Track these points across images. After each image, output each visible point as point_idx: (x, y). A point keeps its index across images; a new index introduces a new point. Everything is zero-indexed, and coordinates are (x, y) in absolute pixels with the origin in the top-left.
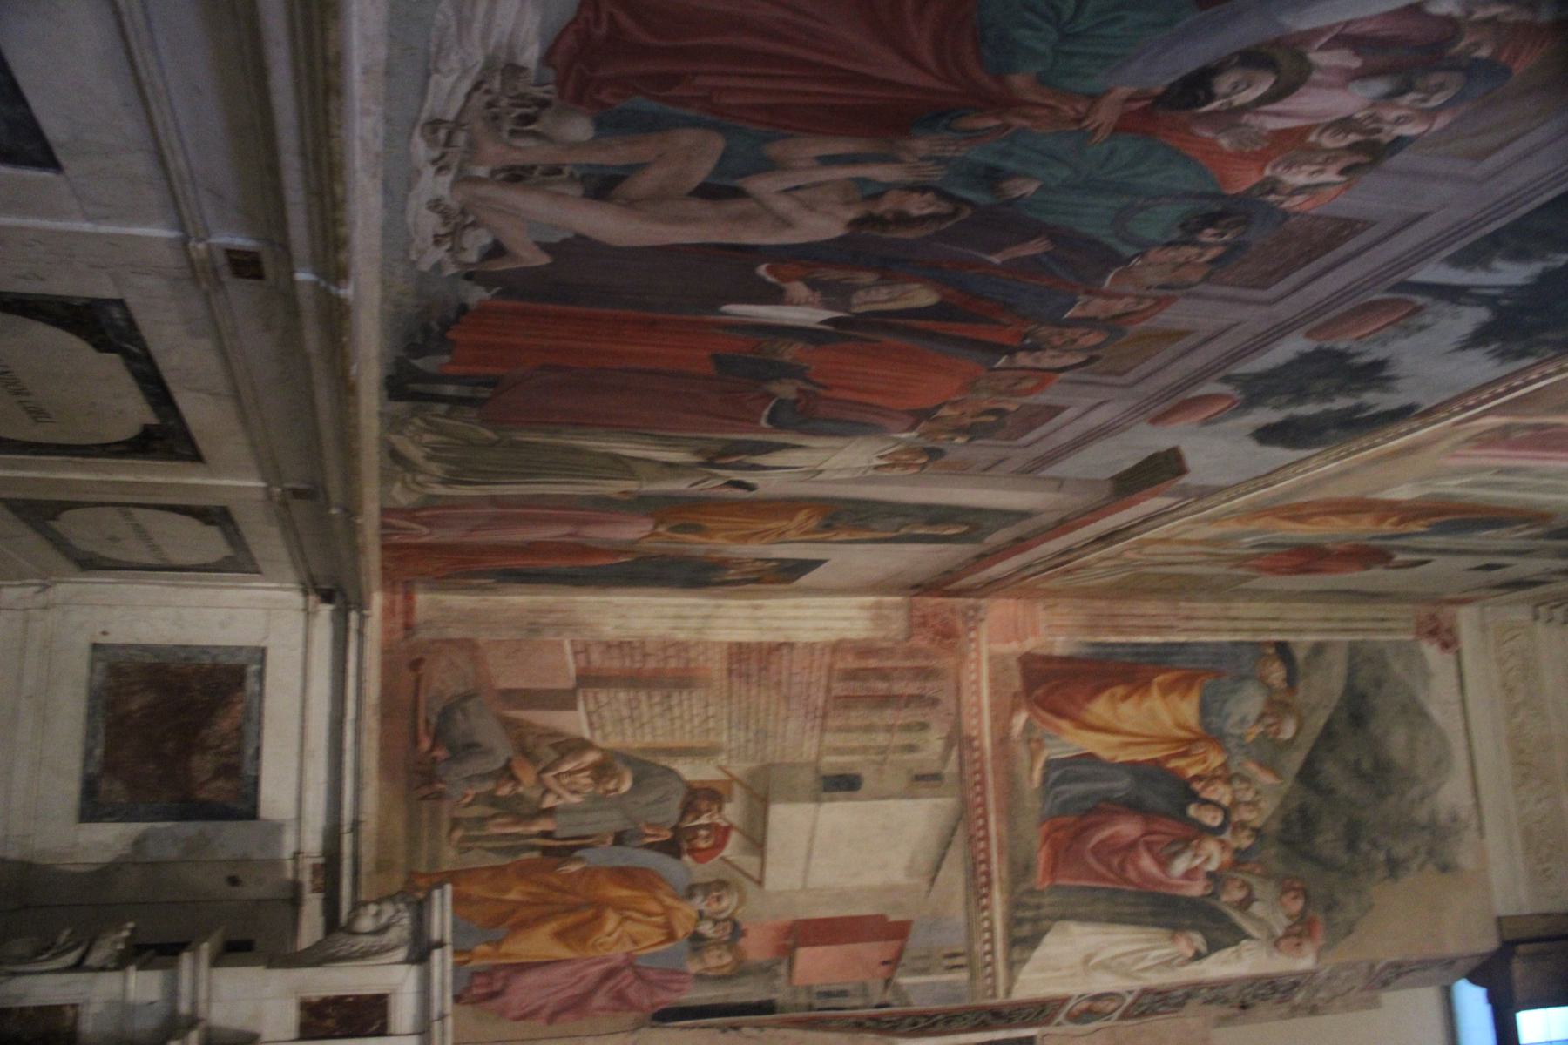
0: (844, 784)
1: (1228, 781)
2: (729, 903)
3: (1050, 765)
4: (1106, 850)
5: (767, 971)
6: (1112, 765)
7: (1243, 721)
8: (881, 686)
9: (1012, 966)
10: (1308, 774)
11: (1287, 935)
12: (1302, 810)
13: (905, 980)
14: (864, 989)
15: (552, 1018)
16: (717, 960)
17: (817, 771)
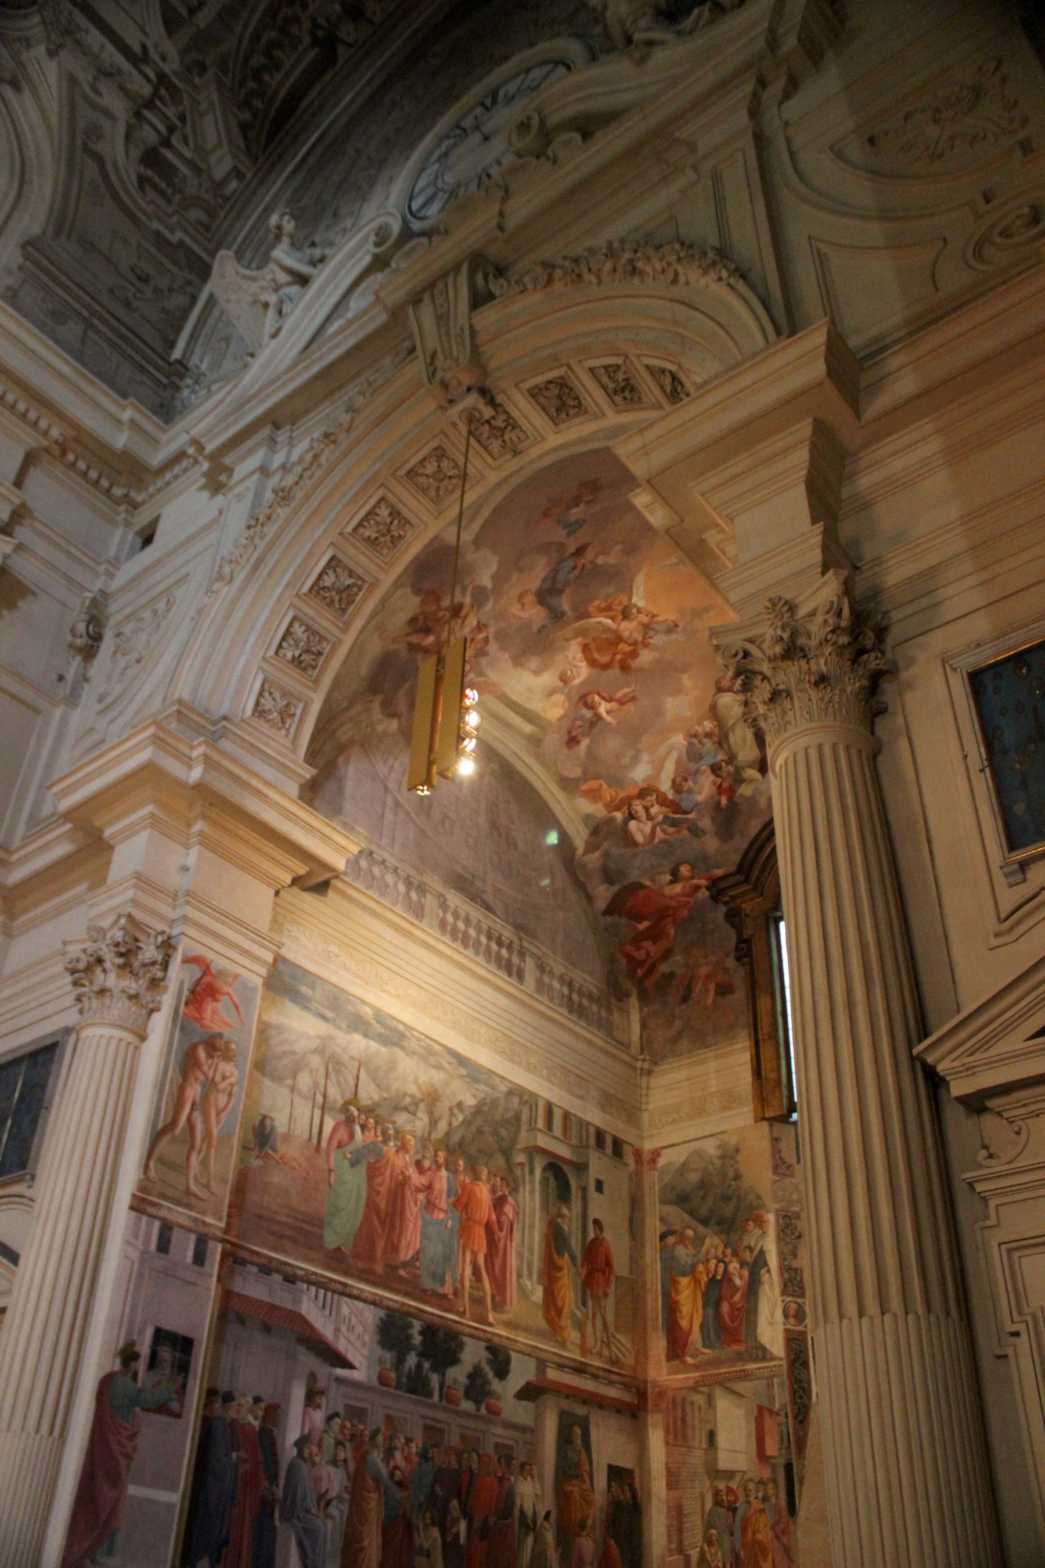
0: (712, 1436)
1: (708, 1260)
2: (751, 1486)
3: (704, 1346)
5: (774, 1468)
8: (679, 1423)
9: (773, 1358)
10: (705, 1222)
11: (761, 1228)
12: (718, 1224)
13: (777, 1406)
16: (771, 1492)
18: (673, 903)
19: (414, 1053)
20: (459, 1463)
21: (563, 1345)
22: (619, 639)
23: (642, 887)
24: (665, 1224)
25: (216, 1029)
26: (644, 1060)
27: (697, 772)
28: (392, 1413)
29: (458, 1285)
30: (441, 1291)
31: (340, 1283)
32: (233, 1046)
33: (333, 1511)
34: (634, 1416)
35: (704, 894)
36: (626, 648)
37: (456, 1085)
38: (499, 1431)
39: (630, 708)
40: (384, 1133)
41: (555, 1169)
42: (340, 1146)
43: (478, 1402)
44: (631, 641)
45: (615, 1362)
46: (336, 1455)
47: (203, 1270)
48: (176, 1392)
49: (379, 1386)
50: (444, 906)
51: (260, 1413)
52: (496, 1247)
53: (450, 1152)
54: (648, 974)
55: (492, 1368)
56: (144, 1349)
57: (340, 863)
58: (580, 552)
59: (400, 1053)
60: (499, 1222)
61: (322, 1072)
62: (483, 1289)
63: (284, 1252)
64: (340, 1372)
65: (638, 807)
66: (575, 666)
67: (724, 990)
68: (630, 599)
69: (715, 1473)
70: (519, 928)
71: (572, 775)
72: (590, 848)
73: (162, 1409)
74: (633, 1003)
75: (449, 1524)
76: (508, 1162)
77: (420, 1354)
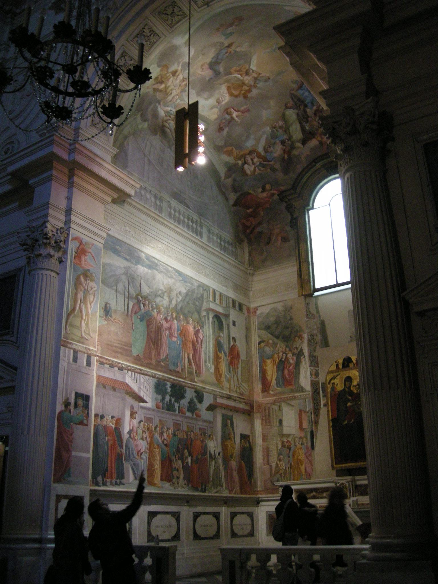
0: (281, 421)
1: (279, 353)
2: (297, 439)
3: (277, 387)
4: (289, 376)
5: (306, 432)
6: (277, 376)
7: (270, 351)
8: (267, 416)
10: (277, 337)
11: (301, 340)
13: (307, 409)
14: (308, 416)
15: (312, 465)
16: (305, 441)
17: (279, 427)
18: (262, 201)
19: (162, 272)
20: (187, 436)
21: (222, 388)
22: (243, 84)
23: (248, 193)
24: (261, 338)
25: (87, 268)
26: (251, 269)
27: (275, 143)
28: (162, 419)
29: (183, 367)
30: (177, 370)
31: (139, 369)
32: (94, 275)
33: (143, 456)
34: (249, 415)
35: (276, 197)
36: (246, 88)
37: (178, 284)
38: (201, 423)
39: (247, 114)
40: (152, 307)
41: (217, 317)
42: (136, 313)
43: (193, 413)
44: (248, 85)
45: (242, 394)
46: (143, 436)
47: (90, 368)
48: (85, 416)
49: (156, 409)
50: (170, 207)
51: (114, 422)
52: (196, 351)
53: (177, 313)
54: (251, 232)
55: (197, 399)
56: (72, 401)
57: (132, 192)
58: (229, 46)
59: (156, 272)
60: (197, 341)
61: (127, 283)
62: (193, 369)
63: (118, 358)
64: (142, 404)
65: (248, 158)
66: (224, 96)
67: (285, 240)
68: (250, 66)
69: (282, 435)
70: (200, 214)
71: (220, 144)
72: (227, 176)
73: (81, 423)
74: (246, 245)
75: (184, 459)
76: (199, 316)
77: (170, 396)
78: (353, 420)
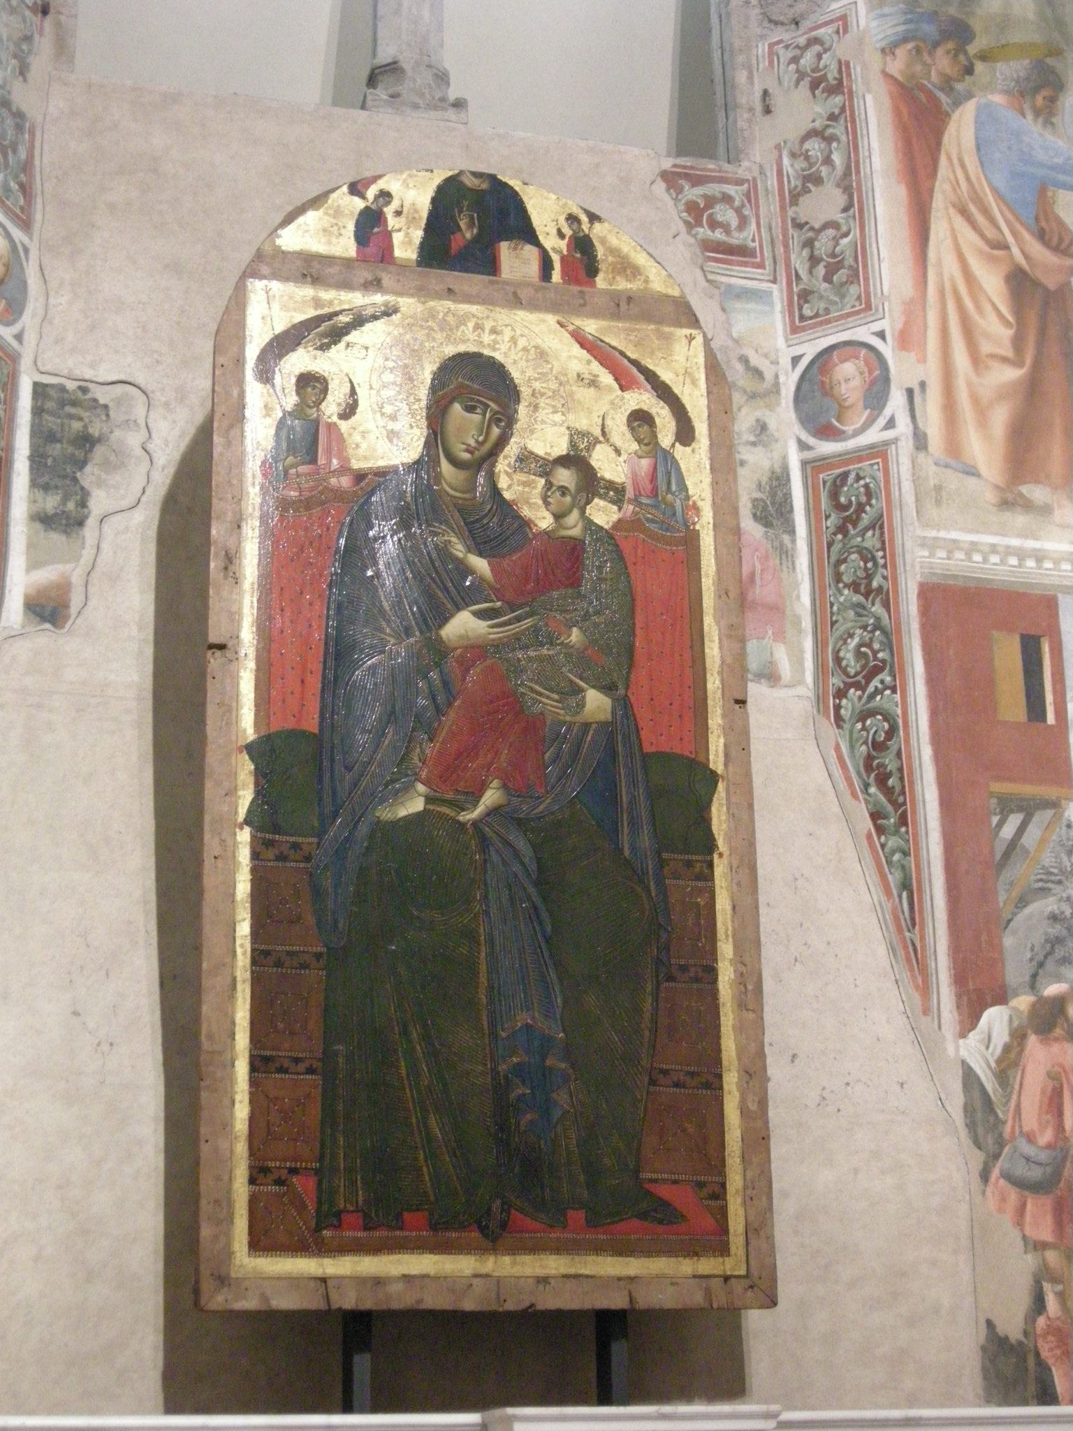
78: (491, 797)
